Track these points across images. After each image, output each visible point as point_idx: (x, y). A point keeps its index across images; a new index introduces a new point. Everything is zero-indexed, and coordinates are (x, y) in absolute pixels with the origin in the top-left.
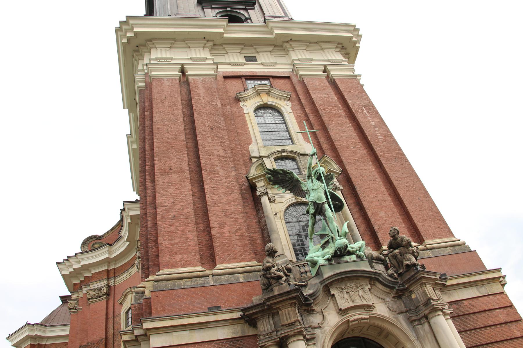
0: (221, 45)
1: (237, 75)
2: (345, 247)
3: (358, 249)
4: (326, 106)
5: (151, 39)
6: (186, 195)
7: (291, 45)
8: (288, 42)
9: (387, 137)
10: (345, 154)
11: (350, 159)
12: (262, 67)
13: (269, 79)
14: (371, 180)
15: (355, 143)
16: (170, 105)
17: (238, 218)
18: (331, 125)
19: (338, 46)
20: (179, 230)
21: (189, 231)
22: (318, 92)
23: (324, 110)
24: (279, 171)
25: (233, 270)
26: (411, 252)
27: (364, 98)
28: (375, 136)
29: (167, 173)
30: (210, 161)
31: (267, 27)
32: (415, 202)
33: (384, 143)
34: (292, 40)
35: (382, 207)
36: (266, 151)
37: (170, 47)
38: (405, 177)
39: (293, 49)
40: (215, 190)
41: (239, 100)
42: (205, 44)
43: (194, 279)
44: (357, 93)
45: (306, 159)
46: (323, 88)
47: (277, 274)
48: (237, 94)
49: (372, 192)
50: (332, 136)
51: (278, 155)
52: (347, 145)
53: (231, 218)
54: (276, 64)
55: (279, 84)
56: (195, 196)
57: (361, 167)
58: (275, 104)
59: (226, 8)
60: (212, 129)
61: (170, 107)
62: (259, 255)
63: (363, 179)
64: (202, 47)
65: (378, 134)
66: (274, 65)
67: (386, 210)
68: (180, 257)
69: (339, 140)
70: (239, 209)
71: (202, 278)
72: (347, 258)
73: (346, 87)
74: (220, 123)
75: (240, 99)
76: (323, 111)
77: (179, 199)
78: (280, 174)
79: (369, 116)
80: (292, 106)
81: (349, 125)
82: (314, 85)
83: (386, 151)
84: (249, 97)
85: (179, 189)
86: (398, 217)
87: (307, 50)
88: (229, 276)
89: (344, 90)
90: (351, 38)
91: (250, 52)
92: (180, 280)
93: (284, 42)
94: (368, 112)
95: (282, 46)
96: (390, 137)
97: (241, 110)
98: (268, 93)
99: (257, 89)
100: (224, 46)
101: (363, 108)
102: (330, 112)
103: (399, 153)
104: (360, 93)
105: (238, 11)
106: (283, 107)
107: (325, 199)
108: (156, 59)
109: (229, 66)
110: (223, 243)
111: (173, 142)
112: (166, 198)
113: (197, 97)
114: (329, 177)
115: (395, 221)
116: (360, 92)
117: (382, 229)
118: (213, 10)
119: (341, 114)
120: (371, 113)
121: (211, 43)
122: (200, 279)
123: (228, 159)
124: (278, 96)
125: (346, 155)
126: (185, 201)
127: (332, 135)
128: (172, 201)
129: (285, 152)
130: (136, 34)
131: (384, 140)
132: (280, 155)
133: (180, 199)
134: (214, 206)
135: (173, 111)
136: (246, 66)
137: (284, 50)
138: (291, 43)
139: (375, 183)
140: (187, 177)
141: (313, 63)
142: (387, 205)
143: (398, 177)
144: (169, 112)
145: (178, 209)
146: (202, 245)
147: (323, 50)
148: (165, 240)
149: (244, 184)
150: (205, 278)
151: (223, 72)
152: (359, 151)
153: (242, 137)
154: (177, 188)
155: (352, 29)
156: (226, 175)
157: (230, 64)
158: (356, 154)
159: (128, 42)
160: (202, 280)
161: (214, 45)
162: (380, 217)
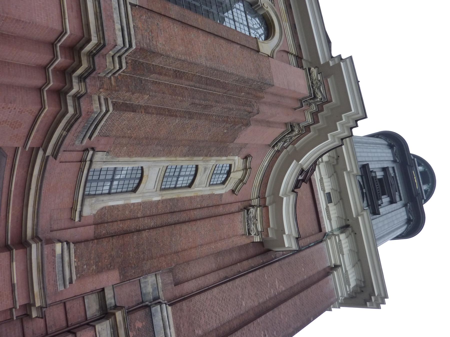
0: (335, 172)
8: (353, 231)
12: (325, 207)
31: (362, 212)
39: (347, 237)
59: (365, 188)
100: (335, 174)
105: (365, 199)
109: (319, 178)
121: (335, 163)
136: (322, 192)
147: (354, 266)
155: (383, 295)
161: (334, 166)
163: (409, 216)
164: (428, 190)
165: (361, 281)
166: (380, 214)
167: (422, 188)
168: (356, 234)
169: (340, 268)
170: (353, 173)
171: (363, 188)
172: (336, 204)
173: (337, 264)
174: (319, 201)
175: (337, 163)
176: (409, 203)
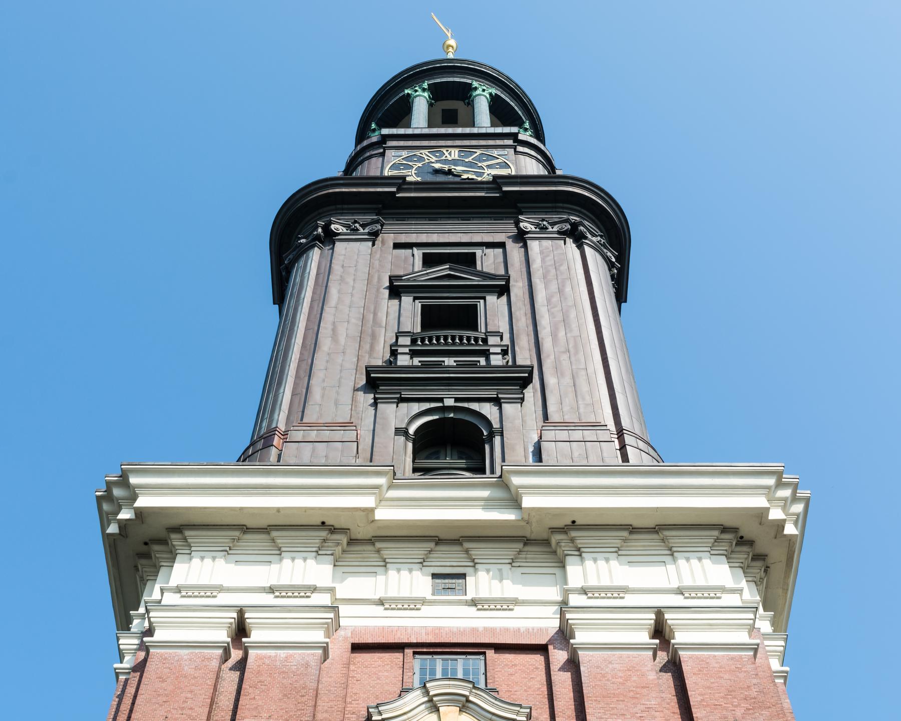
5: (182, 525)
7: (572, 540)
13: (484, 653)
22: (613, 708)
34: (576, 524)
37: (228, 549)
42: (325, 541)
46: (631, 694)
55: (511, 671)
59: (441, 400)
64: (314, 549)
73: (709, 688)
82: (608, 680)
89: (699, 698)
91: (448, 560)
93: (554, 530)
95: (546, 542)
98: (464, 706)
99: (431, 693)
100: (379, 545)
104: (751, 712)
105: (474, 406)
108: (178, 590)
116: (754, 708)
118: (403, 406)
124: (490, 716)
130: (141, 514)
136: (426, 610)
137: (555, 552)
138: (573, 534)
141: (630, 600)
157: (381, 602)
159: (120, 534)
163: (559, 232)
164: (491, 94)
165: (717, 540)
166: (532, 367)
167: (483, 131)
168: (574, 522)
169: (667, 616)
170: (385, 488)
171: (440, 405)
172: (473, 561)
173: (653, 622)
176: (517, 223)
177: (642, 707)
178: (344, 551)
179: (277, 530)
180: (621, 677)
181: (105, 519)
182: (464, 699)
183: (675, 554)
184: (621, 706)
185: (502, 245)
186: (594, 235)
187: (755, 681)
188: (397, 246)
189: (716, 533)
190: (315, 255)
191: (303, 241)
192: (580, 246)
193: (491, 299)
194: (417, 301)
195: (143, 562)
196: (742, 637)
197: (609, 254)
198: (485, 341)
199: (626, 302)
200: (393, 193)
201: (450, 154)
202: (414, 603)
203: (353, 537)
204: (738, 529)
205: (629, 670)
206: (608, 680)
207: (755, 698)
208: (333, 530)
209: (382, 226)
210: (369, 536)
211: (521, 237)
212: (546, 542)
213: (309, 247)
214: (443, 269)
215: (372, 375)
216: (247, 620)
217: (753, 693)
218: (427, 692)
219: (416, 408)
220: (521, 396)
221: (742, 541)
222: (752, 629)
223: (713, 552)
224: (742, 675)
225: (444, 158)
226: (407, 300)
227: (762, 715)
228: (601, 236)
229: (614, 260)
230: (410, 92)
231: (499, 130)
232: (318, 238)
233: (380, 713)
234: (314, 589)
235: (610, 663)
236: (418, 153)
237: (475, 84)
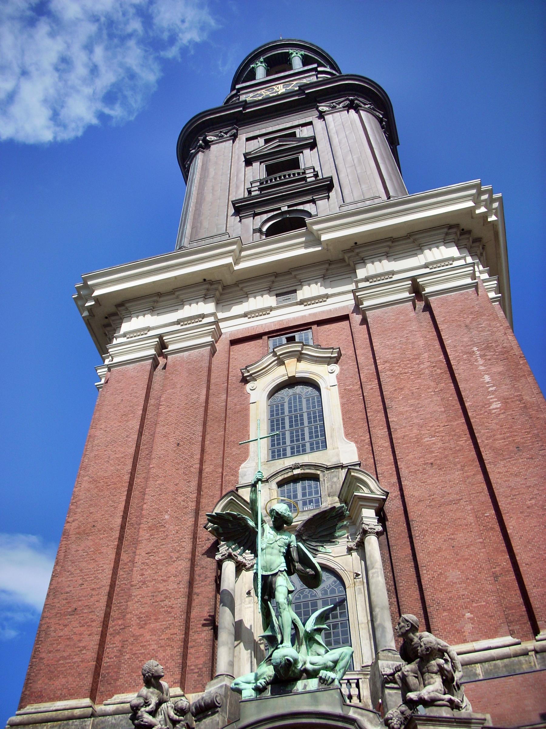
1: (253, 333)
2: (285, 663)
3: (331, 664)
4: (398, 361)
6: (103, 570)
9: (512, 401)
10: (408, 456)
11: (416, 465)
14: (450, 503)
15: (436, 429)
16: (124, 412)
17: (173, 606)
18: (396, 398)
19: (451, 231)
20: (75, 634)
21: (89, 635)
22: (389, 336)
23: (391, 370)
24: (227, 517)
25: (123, 707)
26: (436, 669)
27: (481, 327)
28: (486, 404)
29: (87, 533)
30: (159, 504)
32: (539, 541)
33: (502, 416)
34: (358, 244)
35: (458, 560)
36: (267, 469)
38: (530, 487)
40: (150, 557)
41: (247, 380)
43: (65, 722)
44: (468, 321)
45: (336, 476)
47: (145, 720)
48: (242, 371)
49: (443, 529)
50: (393, 421)
51: (286, 476)
52: (418, 435)
53: (163, 607)
54: (327, 296)
56: (124, 570)
57: (436, 477)
58: (308, 375)
59: (279, 209)
60: (178, 444)
61: (124, 415)
62: (198, 674)
63: (433, 503)
65: (491, 400)
66: (266, 311)
67: (464, 567)
68: (64, 680)
69: (405, 427)
70: (180, 588)
71: (78, 720)
72: (300, 685)
73: (448, 312)
74: (194, 431)
75: (248, 378)
76: (388, 373)
77: (91, 579)
78: (229, 521)
79: (481, 365)
80: (341, 372)
81: (434, 392)
82: (385, 322)
83: (501, 434)
84: (264, 370)
85: (96, 561)
86: (489, 579)
87: (445, 242)
88: (119, 717)
89: (443, 319)
90: (470, 211)
92: (44, 724)
93: (345, 251)
94: (481, 356)
96: (517, 400)
97: (246, 398)
99: (278, 354)
101: (475, 349)
102: (403, 372)
103: (529, 433)
105: (301, 207)
106: (321, 377)
107: (284, 564)
109: (245, 320)
110: (136, 654)
111: (111, 477)
112: (72, 579)
113: (171, 390)
114: (334, 514)
115: (479, 590)
117: (444, 610)
118: (258, 218)
119: (423, 371)
120: (488, 357)
122: (73, 722)
123: (187, 498)
125: (411, 456)
126: (99, 580)
127: (392, 419)
128: (81, 582)
129: (298, 468)
130: (97, 299)
131: (503, 411)
132: (290, 474)
133: (92, 578)
134: (140, 587)
135: (127, 421)
138: (357, 251)
139: (457, 509)
140: (114, 537)
141: (395, 277)
142: (471, 555)
143: (513, 489)
144: (120, 424)
145: (85, 597)
146: (110, 658)
148: (50, 652)
149: (208, 539)
150: (82, 720)
151: (231, 334)
152: (440, 444)
153: (234, 449)
154: (93, 559)
156: (177, 528)
157: (245, 315)
158: (432, 452)
159: (90, 315)
160: (76, 723)
162: (448, 584)
168: (356, 243)
169: (418, 280)
173: (410, 285)
174: (289, 320)
175: (219, 282)
176: (317, 109)
177: (407, 332)
178: (221, 294)
179: (178, 291)
180: (393, 319)
181: (82, 308)
182: (298, 353)
183: (422, 248)
184: (395, 334)
185: (310, 123)
186: (365, 104)
187: (477, 303)
188: (248, 139)
189: (445, 230)
190: (200, 156)
191: (193, 151)
192: (357, 112)
193: (307, 152)
194: (262, 164)
195: (108, 329)
196: (469, 281)
197: (377, 114)
198: (304, 173)
199: (399, 144)
200: (241, 111)
201: (278, 88)
202: (266, 311)
203: (225, 285)
204: (459, 224)
205: (398, 314)
206: (385, 322)
207: (477, 311)
208: (211, 283)
209: (237, 130)
210: (234, 282)
211: (322, 116)
212: (343, 260)
213: (197, 153)
214: (275, 143)
215: (236, 205)
216: (165, 341)
217: (477, 308)
218: (275, 354)
219: (265, 217)
220: (327, 194)
221: (465, 232)
222: (474, 277)
223: (445, 242)
224: (468, 302)
225: (274, 91)
226: (256, 165)
227: (482, 319)
228: (370, 104)
229: (381, 116)
230: (253, 66)
231: (306, 68)
232: (201, 146)
233: (248, 372)
234: (203, 316)
235: (386, 313)
236: (259, 92)
237: (291, 51)
